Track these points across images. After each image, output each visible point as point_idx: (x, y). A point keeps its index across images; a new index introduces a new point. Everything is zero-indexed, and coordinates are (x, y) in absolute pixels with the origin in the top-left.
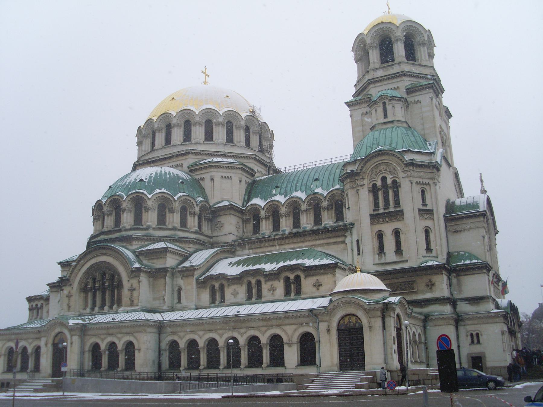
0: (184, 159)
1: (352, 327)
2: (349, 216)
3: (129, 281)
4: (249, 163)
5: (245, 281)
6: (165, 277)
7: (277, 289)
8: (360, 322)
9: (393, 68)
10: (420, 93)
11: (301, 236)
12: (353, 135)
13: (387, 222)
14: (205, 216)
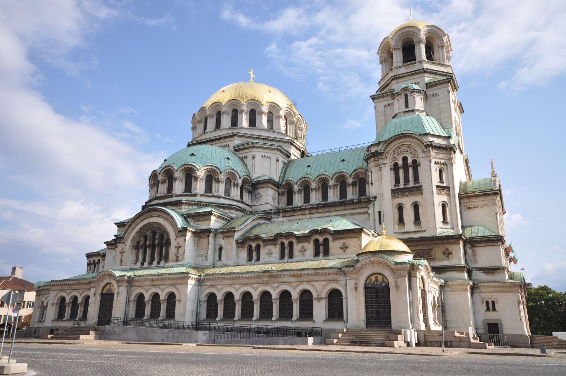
0: (230, 141)
1: (378, 285)
2: (372, 191)
3: (176, 239)
4: (285, 146)
5: (279, 242)
6: (208, 237)
8: (387, 281)
11: (329, 207)
12: (376, 124)
13: (407, 196)
14: (246, 188)
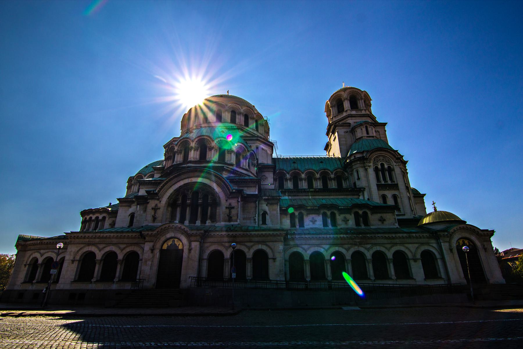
5: (322, 211)
7: (350, 221)
9: (362, 112)
10: (379, 127)
13: (388, 190)
